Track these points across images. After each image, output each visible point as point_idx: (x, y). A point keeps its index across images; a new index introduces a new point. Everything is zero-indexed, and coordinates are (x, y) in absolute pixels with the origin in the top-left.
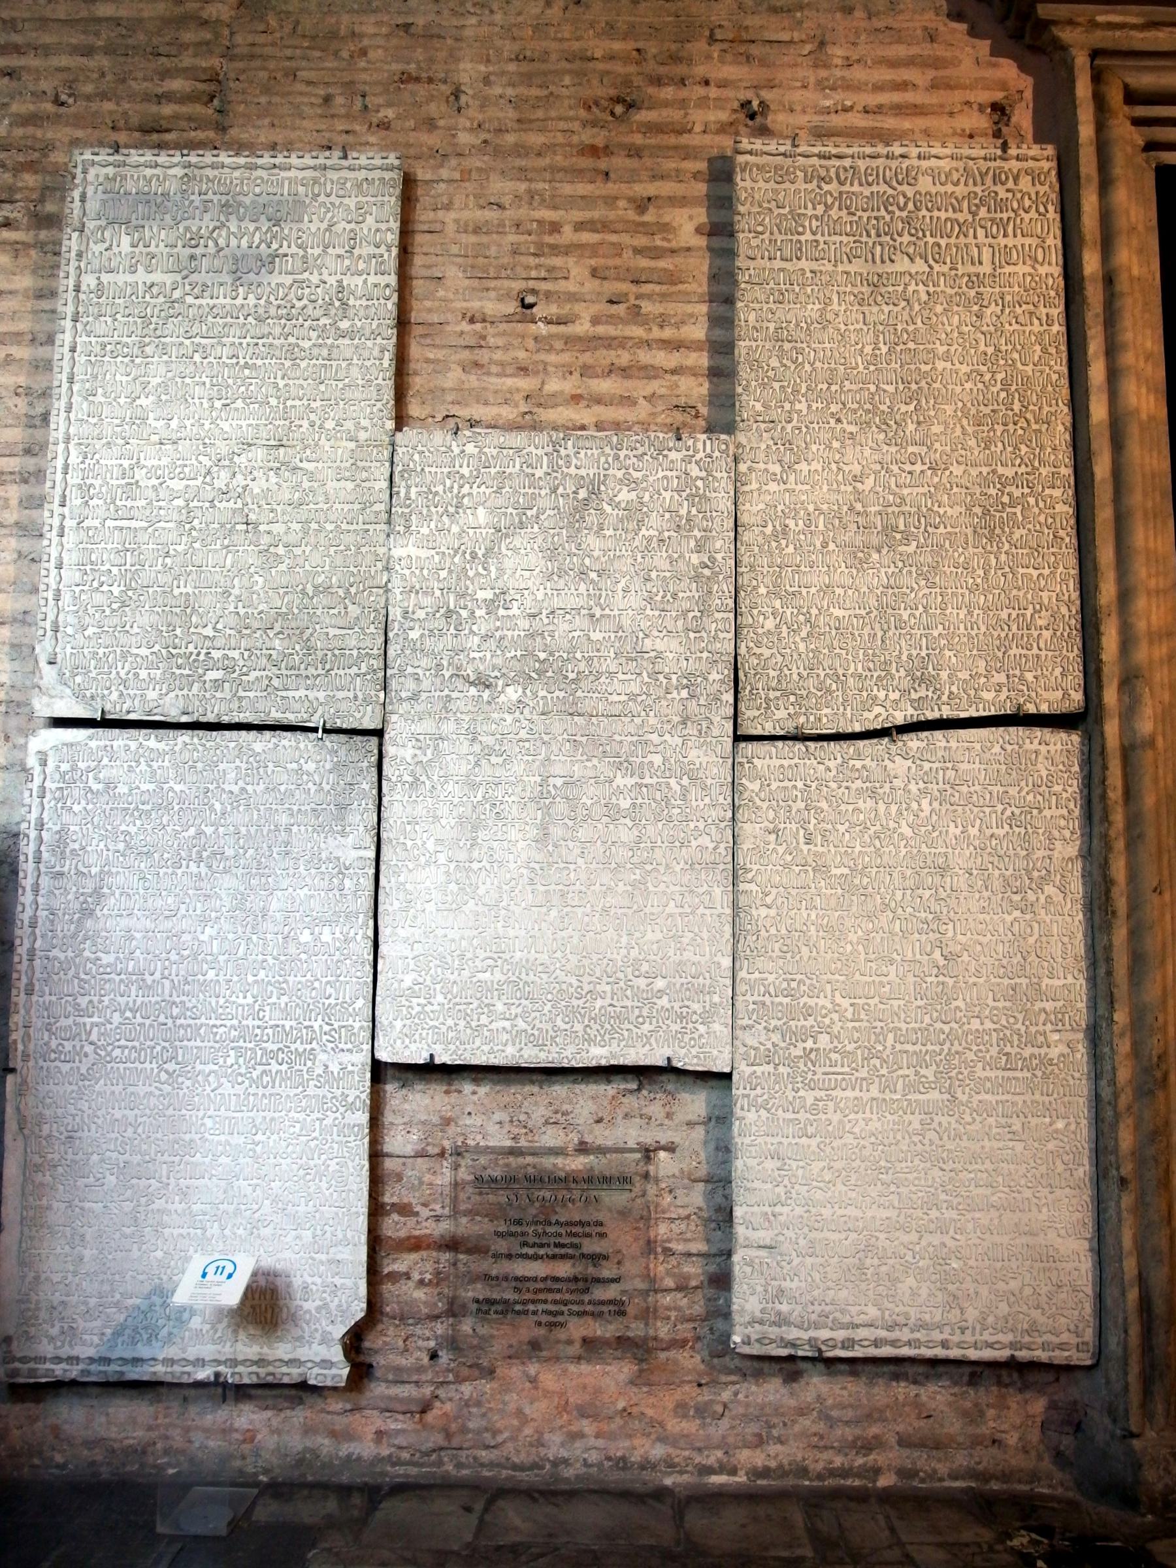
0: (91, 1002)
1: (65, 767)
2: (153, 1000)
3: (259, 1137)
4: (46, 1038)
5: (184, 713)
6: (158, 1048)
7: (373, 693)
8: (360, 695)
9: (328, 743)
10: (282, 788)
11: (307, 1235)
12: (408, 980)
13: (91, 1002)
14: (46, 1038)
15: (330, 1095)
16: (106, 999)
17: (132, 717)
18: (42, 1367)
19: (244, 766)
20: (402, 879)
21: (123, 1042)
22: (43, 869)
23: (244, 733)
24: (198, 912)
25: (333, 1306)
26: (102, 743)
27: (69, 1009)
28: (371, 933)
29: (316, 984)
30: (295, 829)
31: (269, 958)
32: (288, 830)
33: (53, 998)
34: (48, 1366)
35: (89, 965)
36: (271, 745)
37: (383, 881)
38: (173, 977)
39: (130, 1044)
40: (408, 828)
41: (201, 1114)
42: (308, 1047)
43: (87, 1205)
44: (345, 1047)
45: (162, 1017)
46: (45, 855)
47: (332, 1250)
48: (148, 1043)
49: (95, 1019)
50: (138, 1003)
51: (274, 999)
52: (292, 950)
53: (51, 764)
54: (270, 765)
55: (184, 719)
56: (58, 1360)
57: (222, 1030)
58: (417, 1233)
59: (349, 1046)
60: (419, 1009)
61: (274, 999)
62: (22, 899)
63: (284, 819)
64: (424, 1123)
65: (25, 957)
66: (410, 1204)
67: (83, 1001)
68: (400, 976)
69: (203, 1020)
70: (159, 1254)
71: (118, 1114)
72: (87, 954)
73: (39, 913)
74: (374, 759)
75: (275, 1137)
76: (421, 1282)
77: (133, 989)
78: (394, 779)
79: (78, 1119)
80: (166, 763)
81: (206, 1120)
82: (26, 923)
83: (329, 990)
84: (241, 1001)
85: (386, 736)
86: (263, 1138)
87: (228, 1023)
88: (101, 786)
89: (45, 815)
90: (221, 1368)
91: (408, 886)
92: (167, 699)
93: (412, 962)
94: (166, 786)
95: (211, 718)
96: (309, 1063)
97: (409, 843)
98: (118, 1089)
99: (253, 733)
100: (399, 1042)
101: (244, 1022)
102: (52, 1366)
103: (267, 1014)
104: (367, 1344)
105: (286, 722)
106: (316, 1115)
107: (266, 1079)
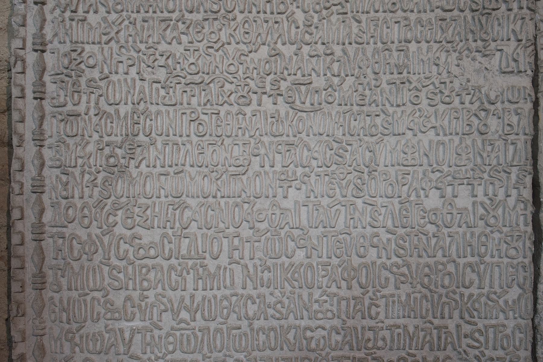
0: (128, 298)
2: (219, 294)
13: (128, 298)
16: (151, 294)
24: (278, 168)
29: (451, 268)
35: (123, 247)
46: (51, 88)
49: (137, 323)
50: (198, 299)
51: (390, 290)
61: (390, 290)
65: (29, 236)
67: (118, 299)
72: (119, 230)
73: (46, 172)
77: (190, 278)
82: (28, 187)
83: (470, 276)
89: (48, 31)
103: (382, 310)
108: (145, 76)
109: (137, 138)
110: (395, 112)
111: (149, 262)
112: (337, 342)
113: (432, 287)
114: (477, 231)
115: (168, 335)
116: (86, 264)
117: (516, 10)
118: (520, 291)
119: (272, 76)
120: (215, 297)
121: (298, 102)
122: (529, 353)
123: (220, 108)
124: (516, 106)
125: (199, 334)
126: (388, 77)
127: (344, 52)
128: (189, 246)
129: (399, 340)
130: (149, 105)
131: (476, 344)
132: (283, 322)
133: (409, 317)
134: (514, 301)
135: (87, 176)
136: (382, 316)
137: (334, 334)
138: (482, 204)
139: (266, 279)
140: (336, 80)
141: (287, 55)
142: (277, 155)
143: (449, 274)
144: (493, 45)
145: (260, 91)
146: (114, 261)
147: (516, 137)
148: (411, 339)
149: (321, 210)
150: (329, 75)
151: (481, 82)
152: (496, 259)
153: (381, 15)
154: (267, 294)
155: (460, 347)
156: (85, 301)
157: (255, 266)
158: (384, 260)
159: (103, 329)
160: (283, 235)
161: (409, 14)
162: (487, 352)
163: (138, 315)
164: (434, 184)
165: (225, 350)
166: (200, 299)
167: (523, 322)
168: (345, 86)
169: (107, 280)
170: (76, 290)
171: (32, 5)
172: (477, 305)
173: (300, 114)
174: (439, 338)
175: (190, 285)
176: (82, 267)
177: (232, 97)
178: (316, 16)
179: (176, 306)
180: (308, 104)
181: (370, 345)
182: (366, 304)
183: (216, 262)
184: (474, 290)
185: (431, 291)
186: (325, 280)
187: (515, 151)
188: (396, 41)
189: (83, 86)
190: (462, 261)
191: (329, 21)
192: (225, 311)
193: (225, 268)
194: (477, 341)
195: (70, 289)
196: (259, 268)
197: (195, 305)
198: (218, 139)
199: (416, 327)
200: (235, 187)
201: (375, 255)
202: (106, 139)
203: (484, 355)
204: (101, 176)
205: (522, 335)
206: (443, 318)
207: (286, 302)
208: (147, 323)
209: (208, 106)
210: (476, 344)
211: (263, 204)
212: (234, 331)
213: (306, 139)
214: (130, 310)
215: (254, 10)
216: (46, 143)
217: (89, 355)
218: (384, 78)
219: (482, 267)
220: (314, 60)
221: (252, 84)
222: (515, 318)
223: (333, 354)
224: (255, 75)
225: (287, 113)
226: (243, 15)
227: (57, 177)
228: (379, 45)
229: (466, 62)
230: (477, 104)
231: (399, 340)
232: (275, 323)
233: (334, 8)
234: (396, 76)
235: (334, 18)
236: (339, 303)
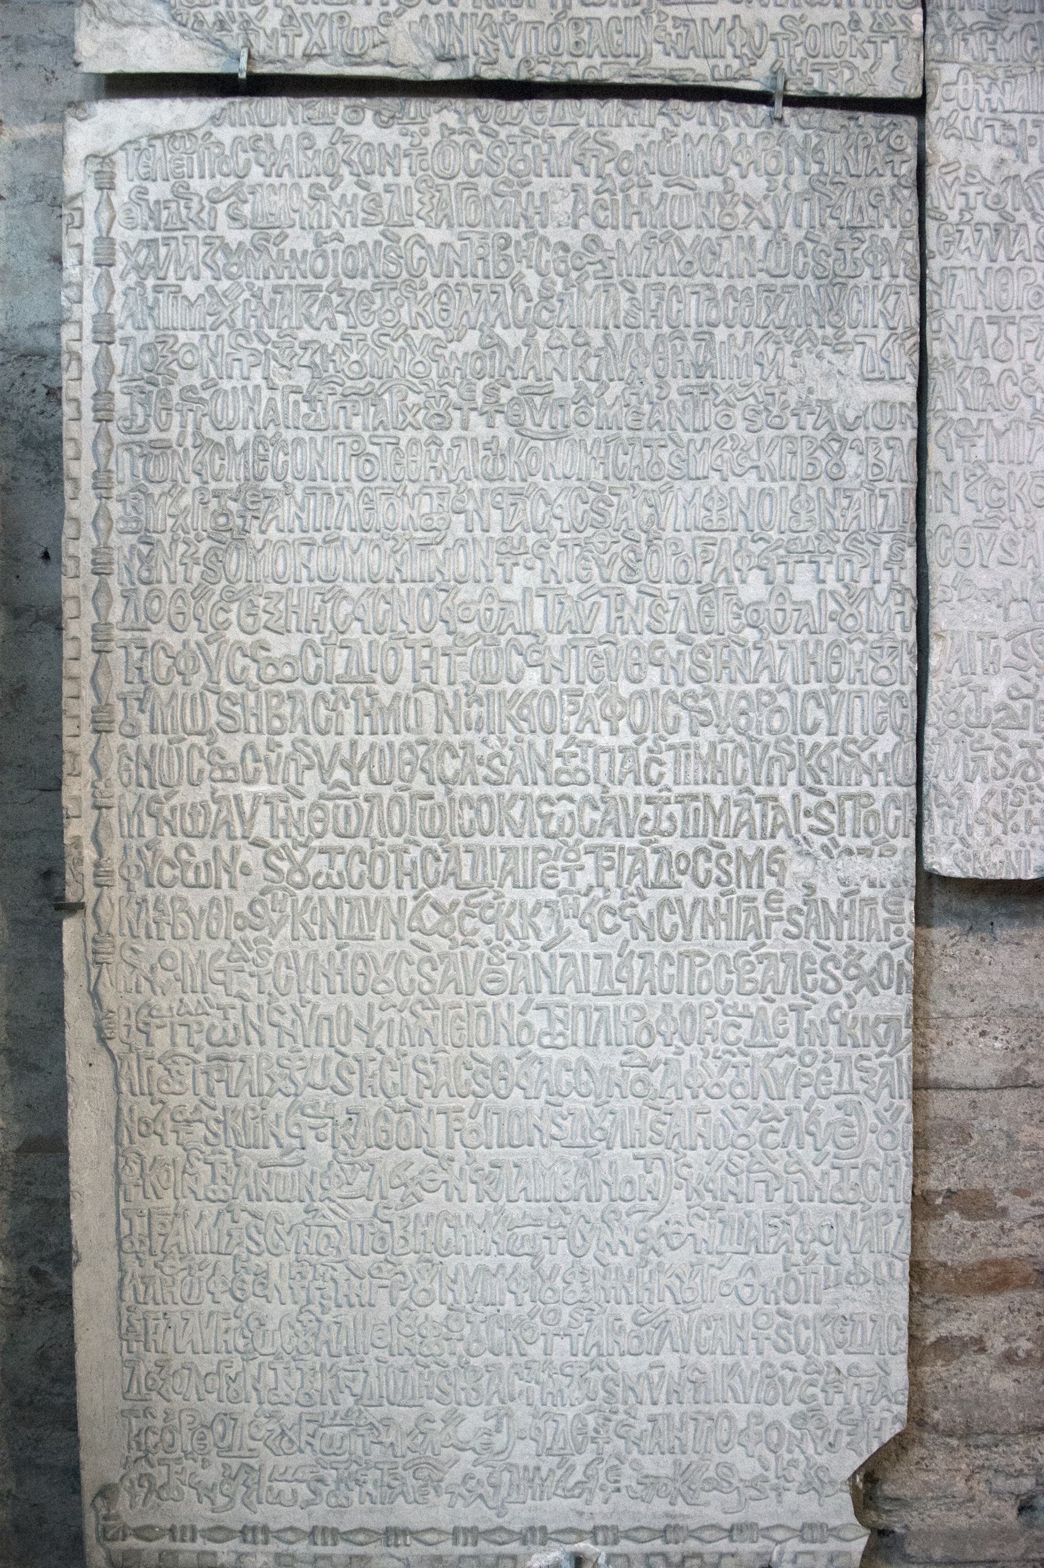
0: (250, 746)
1: (158, 191)
2: (398, 740)
3: (658, 1051)
4: (149, 830)
5: (444, 59)
6: (415, 852)
7: (896, 12)
8: (865, 17)
9: (794, 130)
10: (688, 237)
11: (771, 1265)
12: (999, 687)
13: (250, 746)
14: (149, 830)
15: (819, 955)
16: (285, 739)
17: (318, 68)
18: (189, 1548)
19: (592, 183)
20: (979, 453)
21: (331, 840)
22: (117, 436)
23: (590, 105)
25: (831, 1414)
26: (246, 132)
27: (198, 763)
28: (908, 578)
29: (783, 700)
30: (721, 333)
31: (668, 639)
32: (705, 335)
33: (161, 740)
34: (200, 1544)
36: (656, 135)
37: (935, 458)
38: (443, 686)
39: (348, 844)
40: (991, 331)
41: (518, 1004)
42: (768, 845)
43: (266, 1207)
44: (855, 844)
45: (420, 778)
46: (121, 402)
47: (827, 1297)
48: (391, 840)
49: (262, 788)
50: (362, 749)
51: (684, 735)
52: (725, 618)
53: (124, 186)
54: (657, 180)
55: (442, 72)
56: (219, 1532)
57: (562, 808)
58: (1003, 1253)
59: (865, 842)
60: (1021, 755)
61: (684, 735)
62: (73, 508)
63: (692, 310)
64: (1017, 1012)
65: (87, 644)
66: (987, 1193)
67: (232, 747)
68: (978, 680)
69: (517, 785)
70: (438, 1311)
71: (327, 1006)
72: (233, 634)
74: (907, 169)
75: (694, 1050)
76: (1009, 1358)
77: (349, 714)
78: (954, 216)
79: (234, 1016)
80: (405, 179)
81: (532, 1016)
82: (86, 563)
83: (814, 713)
84: (605, 740)
85: (932, 115)
86: (669, 1053)
87: (577, 793)
88: (246, 235)
89: (117, 305)
90: (584, 1546)
91: (994, 469)
92: (400, 25)
93: (1006, 647)
94: (405, 233)
95: (507, 69)
96: (770, 882)
97: (995, 369)
98: (324, 947)
99: (614, 105)
100: (979, 831)
101: (615, 790)
102: (211, 1546)
103: (668, 770)
104: (888, 1489)
105: (690, 79)
106: (784, 1002)
107: (669, 920)
108: (279, 382)
109: (262, 485)
110: (691, 440)
111: (283, 688)
112: (593, 822)
113: (752, 733)
114: (826, 639)
115: (315, 806)
116: (181, 690)
117: (887, 279)
118: (897, 739)
119: (487, 380)
120: (391, 745)
121: (529, 424)
122: (911, 842)
123: (400, 434)
124: (887, 434)
125: (365, 806)
126: (681, 382)
127: (606, 338)
128: (348, 661)
129: (696, 820)
130: (283, 430)
131: (824, 827)
132: (503, 788)
133: (714, 782)
134: (886, 755)
135: (182, 548)
136: (668, 780)
137: (588, 810)
138: (832, 593)
139: (474, 716)
140: (593, 386)
141: (512, 346)
142: (493, 511)
143: (780, 710)
144: (850, 333)
145: (466, 406)
146: (227, 687)
147: (889, 485)
148: (717, 819)
149: (568, 603)
150: (581, 378)
151: (833, 393)
152: (857, 686)
153: (669, 281)
154: (477, 742)
155: (798, 831)
156: (178, 750)
157: (456, 694)
158: (673, 687)
159: (208, 797)
160: (503, 644)
161: (715, 280)
162: (842, 841)
163: (264, 775)
164: (754, 561)
165: (406, 835)
166: (367, 749)
167: (899, 790)
168: (609, 398)
169: (214, 717)
170: (165, 732)
171: (91, 267)
172: (824, 762)
173: (532, 443)
174: (764, 816)
175: (349, 727)
176: (173, 695)
177: (420, 417)
178: (560, 281)
179: (326, 760)
180: (546, 427)
181: (648, 827)
182: (642, 761)
183: (392, 689)
184: (821, 738)
185: (750, 739)
186: (574, 720)
187: (886, 507)
188: (693, 323)
189: (176, 399)
190: (801, 689)
191: (582, 290)
192: (408, 769)
193: (408, 698)
194: (825, 821)
195: (153, 731)
196: (464, 700)
197: (359, 757)
198: (396, 485)
199: (726, 799)
200: (425, 564)
201: (657, 679)
202: (213, 485)
203: (836, 845)
204: (204, 547)
205: (898, 813)
206: (770, 783)
207: (508, 754)
208: (279, 789)
209: (381, 432)
210: (824, 827)
211: (468, 592)
212: (421, 803)
213: (543, 484)
214: (250, 766)
215: (457, 271)
216: (115, 492)
217: (186, 840)
218: (675, 384)
219: (834, 699)
220: (556, 354)
221: (453, 393)
222: (888, 784)
223: (587, 841)
224: (458, 380)
225: (511, 441)
226: (438, 281)
227: (132, 547)
228: (666, 329)
229: (807, 360)
230: (826, 430)
231: (696, 820)
232: (490, 790)
233: (590, 269)
234: (694, 381)
235: (590, 285)
236: (596, 757)
